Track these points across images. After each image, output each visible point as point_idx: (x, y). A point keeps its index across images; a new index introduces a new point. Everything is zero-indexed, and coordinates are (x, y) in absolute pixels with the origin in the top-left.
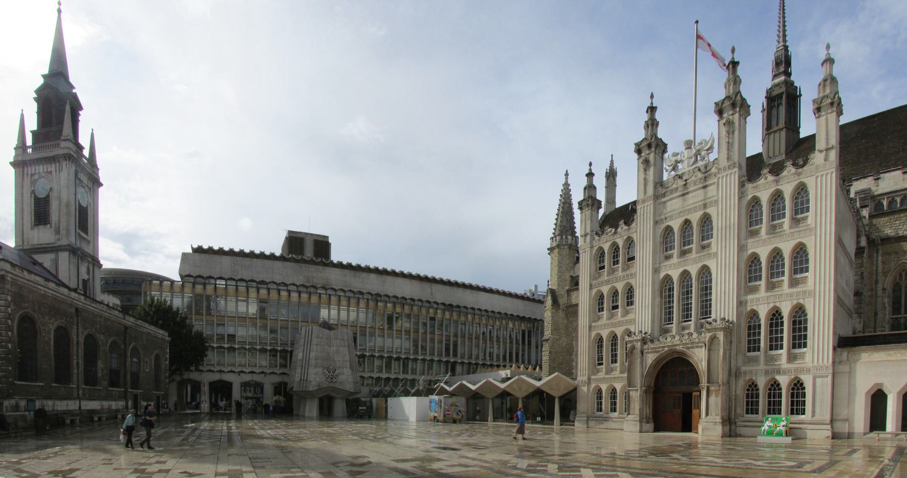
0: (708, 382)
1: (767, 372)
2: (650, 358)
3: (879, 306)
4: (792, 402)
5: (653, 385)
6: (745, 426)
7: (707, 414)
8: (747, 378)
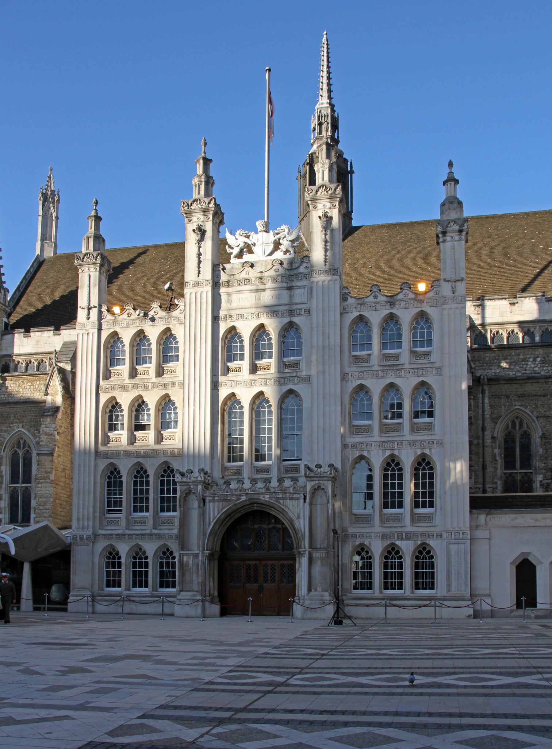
0: (310, 547)
1: (384, 536)
2: (215, 511)
3: (488, 459)
4: (417, 574)
5: (218, 549)
6: (357, 605)
7: (309, 590)
8: (357, 543)
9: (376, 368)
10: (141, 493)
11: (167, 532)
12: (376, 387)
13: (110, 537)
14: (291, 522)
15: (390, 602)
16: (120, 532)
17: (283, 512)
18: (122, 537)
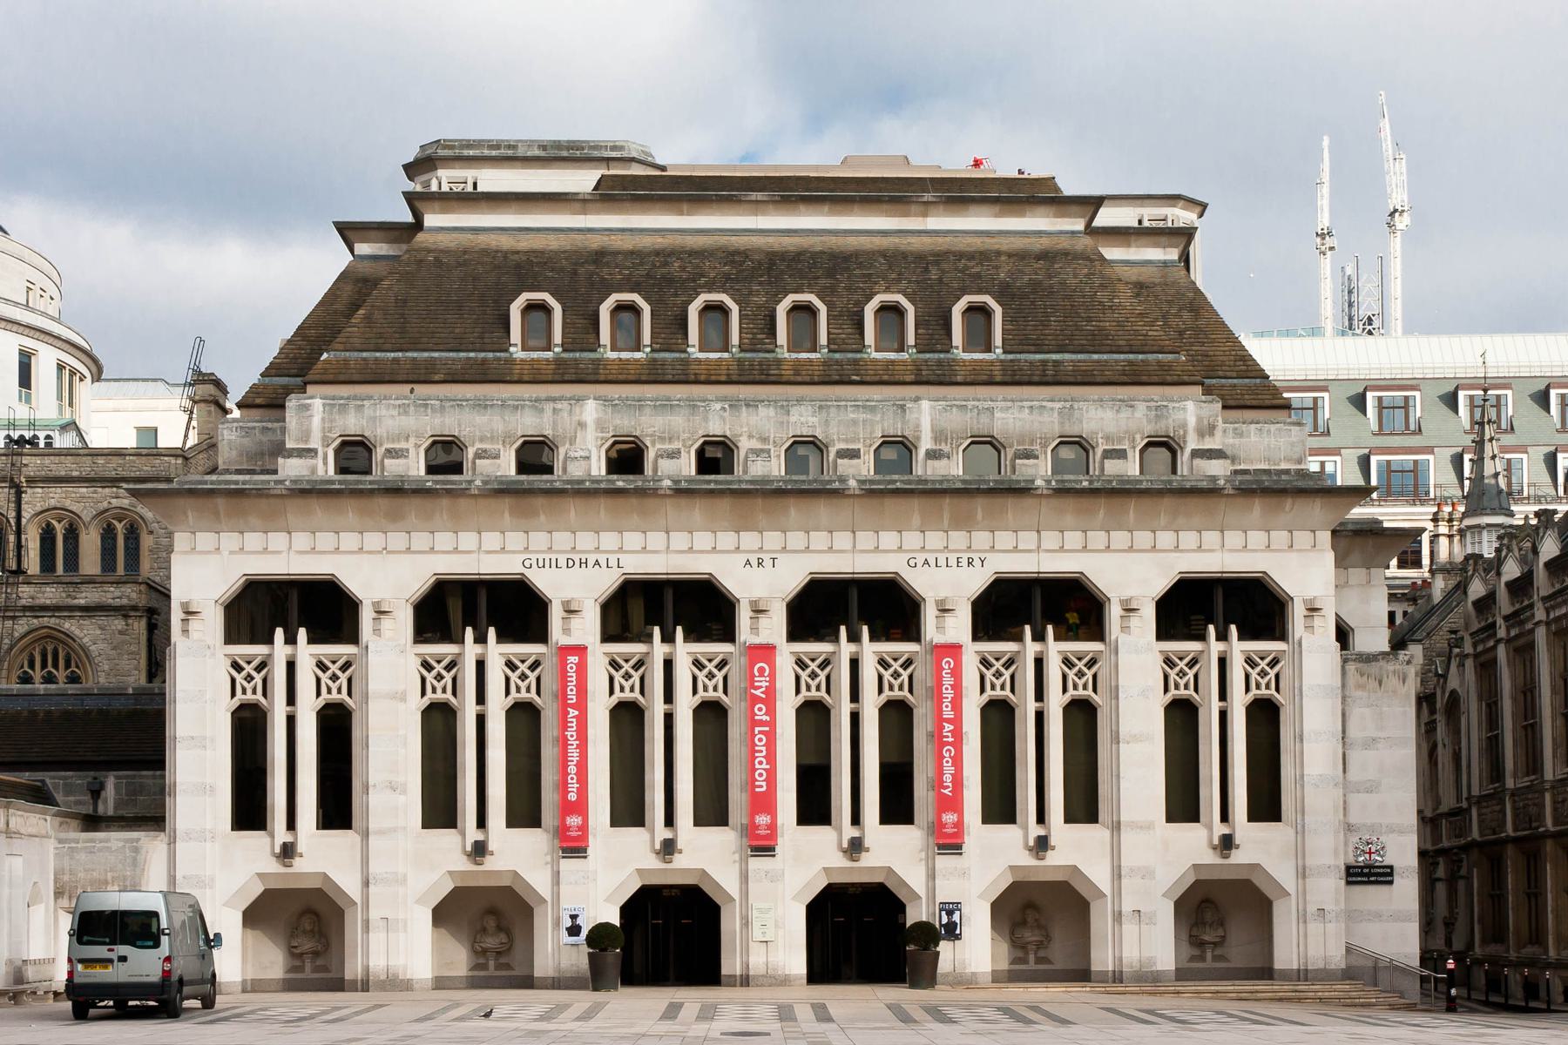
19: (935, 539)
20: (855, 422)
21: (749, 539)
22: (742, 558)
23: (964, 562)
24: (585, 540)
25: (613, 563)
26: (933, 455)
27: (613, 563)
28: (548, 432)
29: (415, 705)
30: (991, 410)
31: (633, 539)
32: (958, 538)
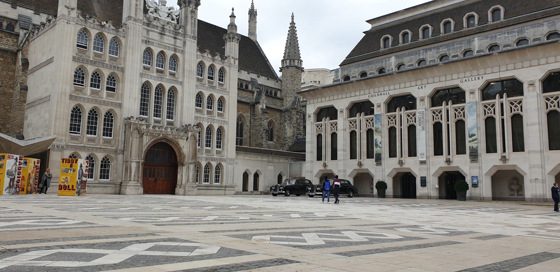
1: (207, 159)
9: (207, 86)
10: (108, 126)
11: (110, 148)
12: (206, 94)
13: (76, 147)
14: (180, 149)
15: (208, 188)
16: (82, 145)
17: (177, 145)
18: (83, 148)
19: (468, 74)
20: (457, 48)
21: (419, 82)
22: (417, 87)
23: (477, 79)
24: (381, 89)
25: (387, 92)
26: (478, 52)
27: (387, 92)
28: (384, 66)
29: (348, 131)
30: (496, 36)
31: (392, 87)
32: (475, 73)
